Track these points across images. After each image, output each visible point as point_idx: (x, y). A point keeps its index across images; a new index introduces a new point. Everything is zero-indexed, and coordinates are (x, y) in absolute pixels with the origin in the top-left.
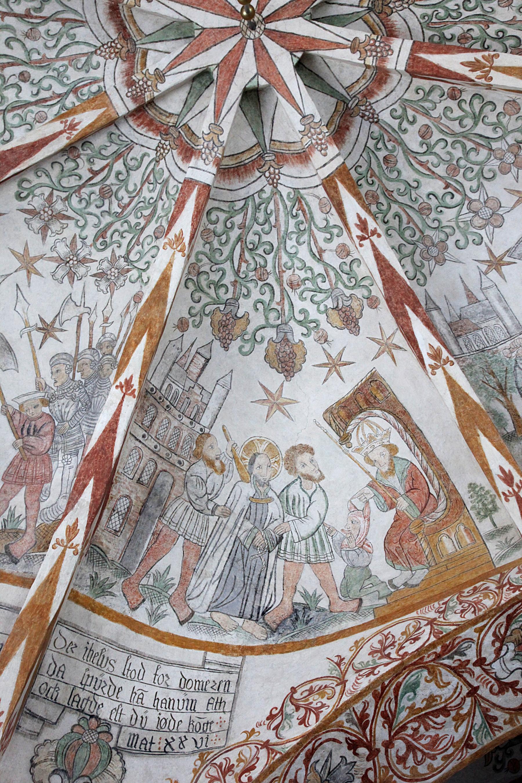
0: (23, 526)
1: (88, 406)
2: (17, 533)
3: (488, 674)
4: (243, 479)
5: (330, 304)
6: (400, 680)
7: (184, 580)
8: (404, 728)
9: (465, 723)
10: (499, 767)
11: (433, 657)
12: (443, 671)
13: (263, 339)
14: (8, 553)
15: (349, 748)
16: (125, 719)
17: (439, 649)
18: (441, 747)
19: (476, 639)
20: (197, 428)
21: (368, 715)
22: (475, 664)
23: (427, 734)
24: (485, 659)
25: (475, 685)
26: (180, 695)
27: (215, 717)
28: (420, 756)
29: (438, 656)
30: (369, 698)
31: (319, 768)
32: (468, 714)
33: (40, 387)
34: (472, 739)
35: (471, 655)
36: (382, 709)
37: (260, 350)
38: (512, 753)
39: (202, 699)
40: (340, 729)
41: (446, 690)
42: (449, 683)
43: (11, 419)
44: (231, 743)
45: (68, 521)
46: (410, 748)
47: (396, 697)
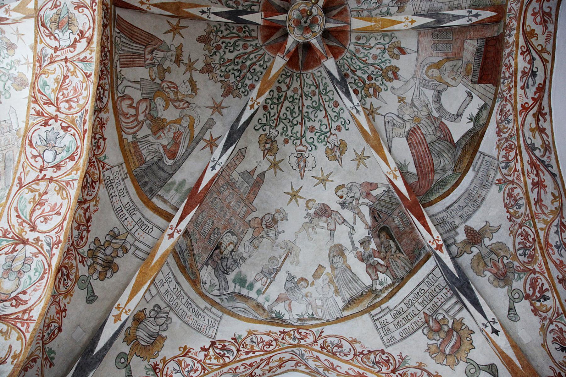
3: (63, 49)
6: (37, 88)
8: (57, 99)
9: (77, 71)
10: (246, 93)
11: (39, 68)
12: (48, 67)
13: (9, 87)
15: (45, 126)
17: (38, 64)
18: (79, 88)
19: (44, 46)
20: (14, 131)
21: (39, 111)
22: (55, 53)
23: (69, 91)
24: (56, 47)
25: (64, 57)
28: (75, 100)
29: (40, 66)
30: (33, 105)
31: (39, 143)
32: (75, 68)
34: (87, 73)
35: (50, 51)
36: (42, 103)
38: (246, 85)
40: (34, 125)
41: (57, 71)
42: (55, 69)
46: (67, 101)
47: (43, 94)
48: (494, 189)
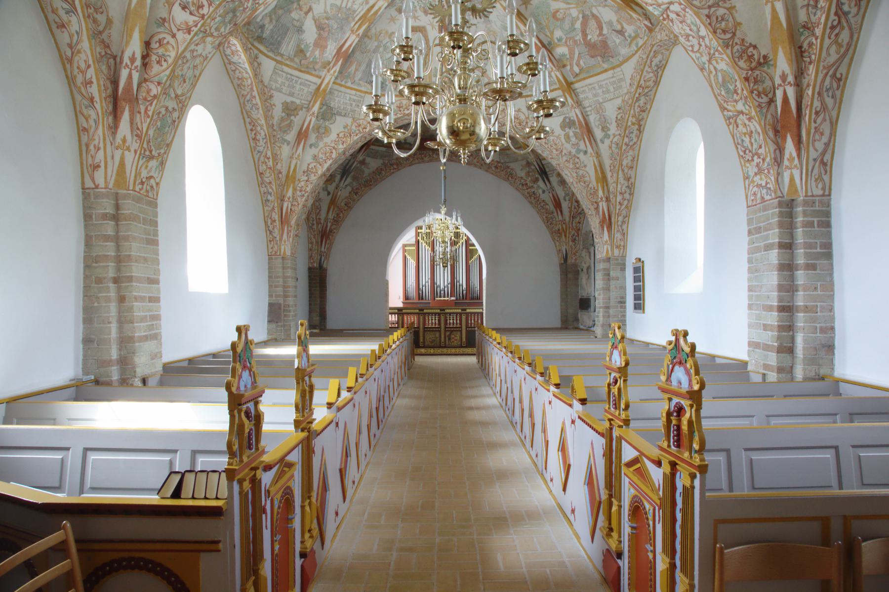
0: (318, 61)
1: (342, 28)
2: (316, 63)
4: (376, 41)
5: (422, 5)
7: (355, 72)
14: (314, 68)
16: (336, 107)
26: (348, 102)
27: (356, 109)
33: (326, 12)
37: (395, 7)
39: (354, 104)
43: (315, 22)
44: (360, 118)
45: (334, 69)
48: (381, 161)
